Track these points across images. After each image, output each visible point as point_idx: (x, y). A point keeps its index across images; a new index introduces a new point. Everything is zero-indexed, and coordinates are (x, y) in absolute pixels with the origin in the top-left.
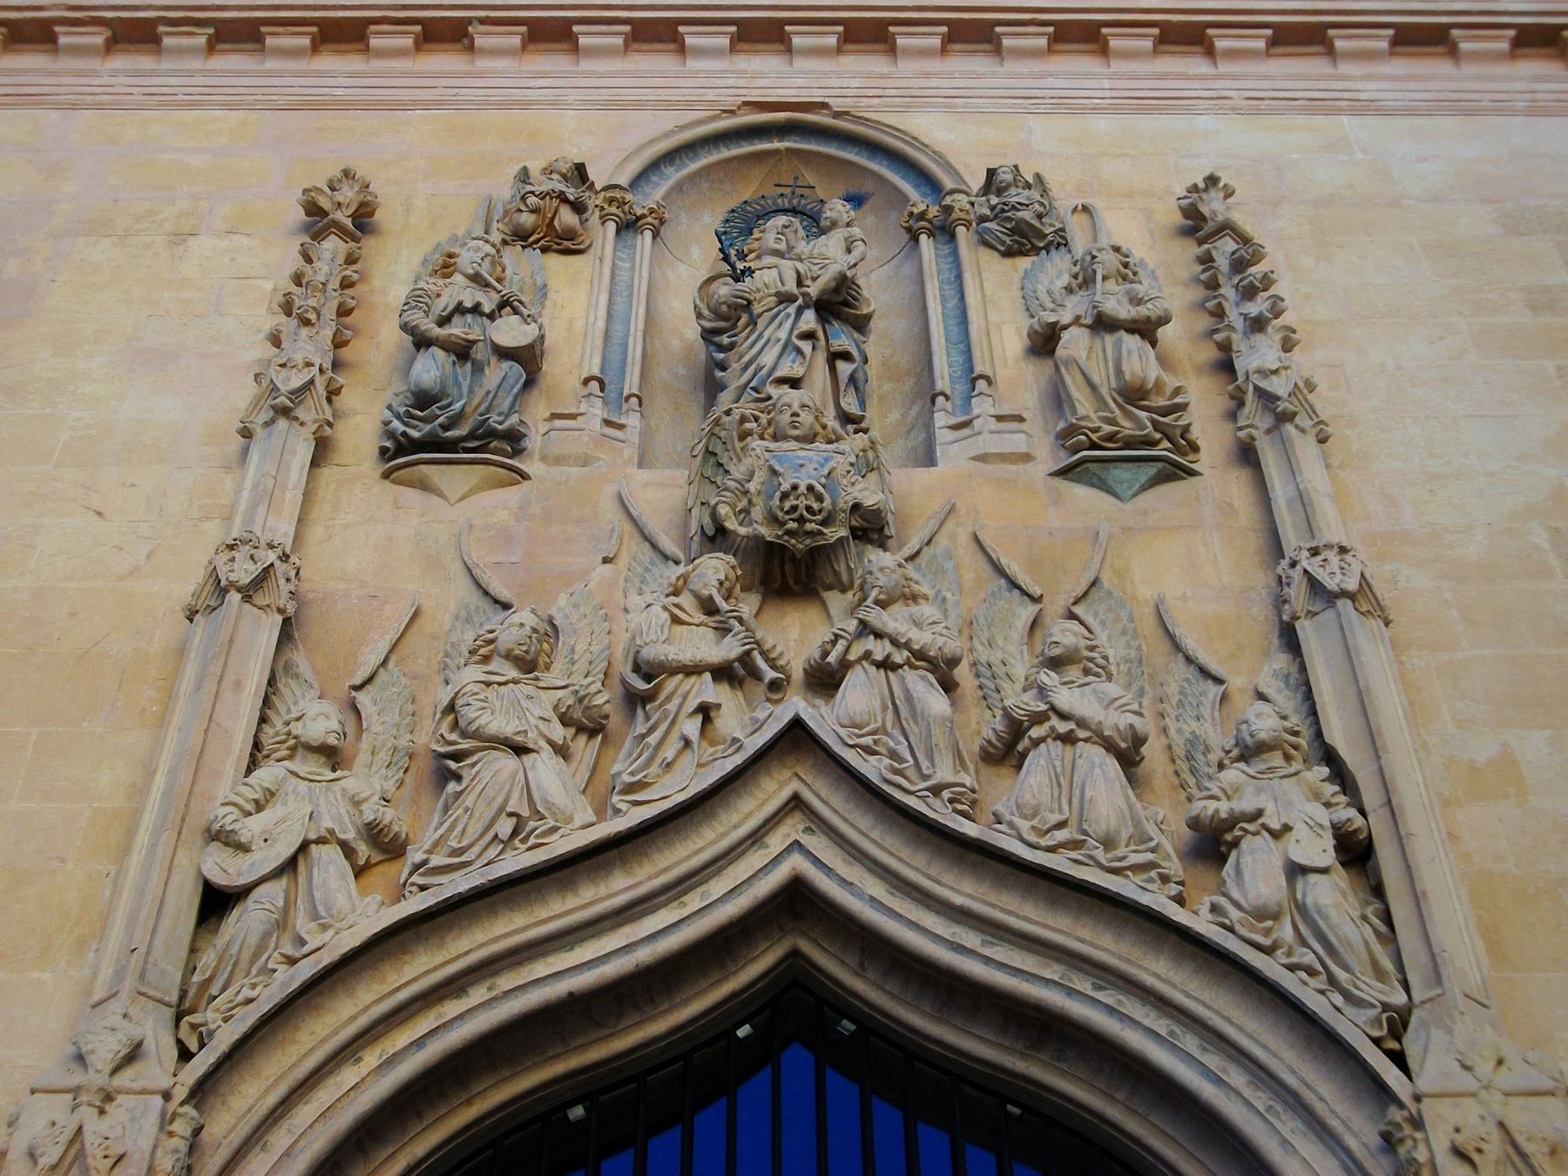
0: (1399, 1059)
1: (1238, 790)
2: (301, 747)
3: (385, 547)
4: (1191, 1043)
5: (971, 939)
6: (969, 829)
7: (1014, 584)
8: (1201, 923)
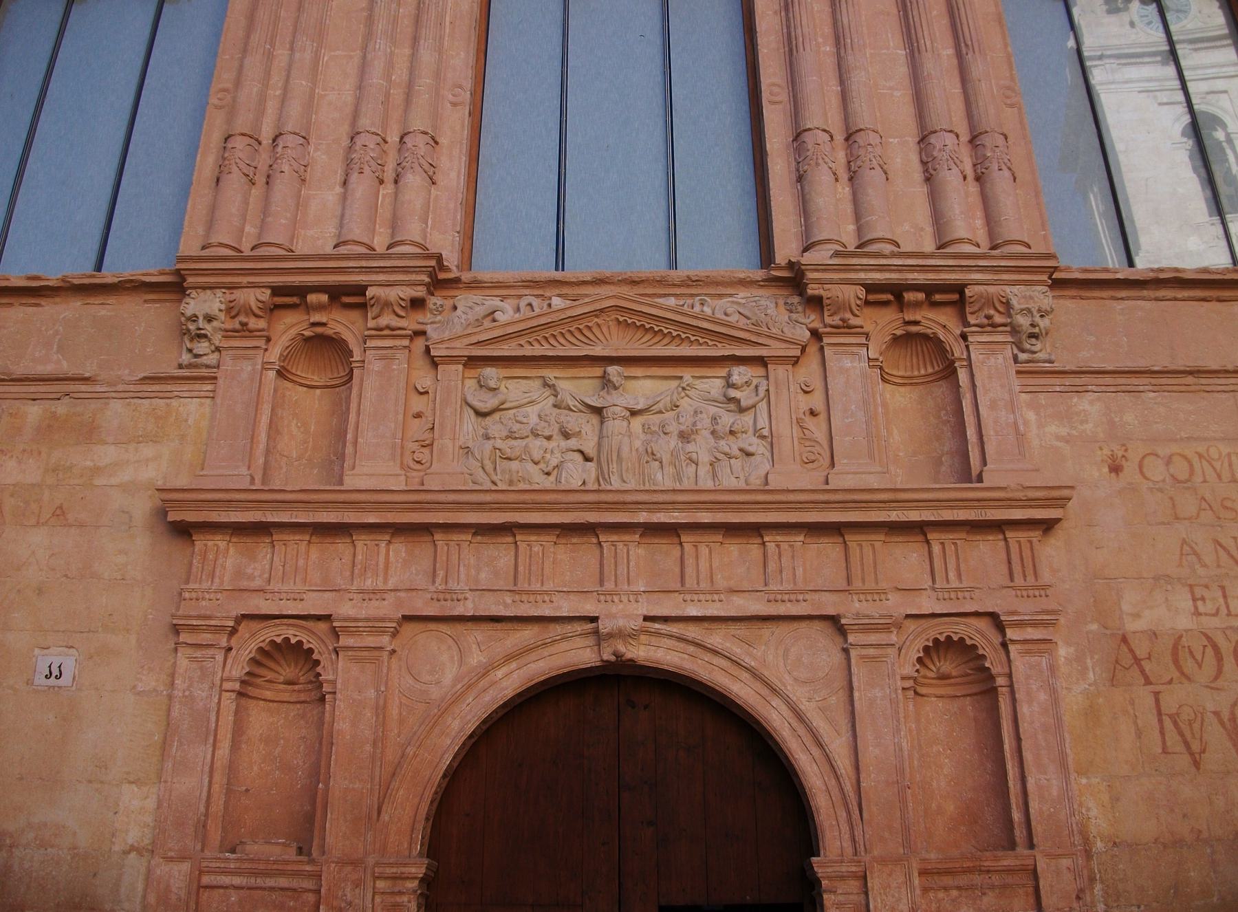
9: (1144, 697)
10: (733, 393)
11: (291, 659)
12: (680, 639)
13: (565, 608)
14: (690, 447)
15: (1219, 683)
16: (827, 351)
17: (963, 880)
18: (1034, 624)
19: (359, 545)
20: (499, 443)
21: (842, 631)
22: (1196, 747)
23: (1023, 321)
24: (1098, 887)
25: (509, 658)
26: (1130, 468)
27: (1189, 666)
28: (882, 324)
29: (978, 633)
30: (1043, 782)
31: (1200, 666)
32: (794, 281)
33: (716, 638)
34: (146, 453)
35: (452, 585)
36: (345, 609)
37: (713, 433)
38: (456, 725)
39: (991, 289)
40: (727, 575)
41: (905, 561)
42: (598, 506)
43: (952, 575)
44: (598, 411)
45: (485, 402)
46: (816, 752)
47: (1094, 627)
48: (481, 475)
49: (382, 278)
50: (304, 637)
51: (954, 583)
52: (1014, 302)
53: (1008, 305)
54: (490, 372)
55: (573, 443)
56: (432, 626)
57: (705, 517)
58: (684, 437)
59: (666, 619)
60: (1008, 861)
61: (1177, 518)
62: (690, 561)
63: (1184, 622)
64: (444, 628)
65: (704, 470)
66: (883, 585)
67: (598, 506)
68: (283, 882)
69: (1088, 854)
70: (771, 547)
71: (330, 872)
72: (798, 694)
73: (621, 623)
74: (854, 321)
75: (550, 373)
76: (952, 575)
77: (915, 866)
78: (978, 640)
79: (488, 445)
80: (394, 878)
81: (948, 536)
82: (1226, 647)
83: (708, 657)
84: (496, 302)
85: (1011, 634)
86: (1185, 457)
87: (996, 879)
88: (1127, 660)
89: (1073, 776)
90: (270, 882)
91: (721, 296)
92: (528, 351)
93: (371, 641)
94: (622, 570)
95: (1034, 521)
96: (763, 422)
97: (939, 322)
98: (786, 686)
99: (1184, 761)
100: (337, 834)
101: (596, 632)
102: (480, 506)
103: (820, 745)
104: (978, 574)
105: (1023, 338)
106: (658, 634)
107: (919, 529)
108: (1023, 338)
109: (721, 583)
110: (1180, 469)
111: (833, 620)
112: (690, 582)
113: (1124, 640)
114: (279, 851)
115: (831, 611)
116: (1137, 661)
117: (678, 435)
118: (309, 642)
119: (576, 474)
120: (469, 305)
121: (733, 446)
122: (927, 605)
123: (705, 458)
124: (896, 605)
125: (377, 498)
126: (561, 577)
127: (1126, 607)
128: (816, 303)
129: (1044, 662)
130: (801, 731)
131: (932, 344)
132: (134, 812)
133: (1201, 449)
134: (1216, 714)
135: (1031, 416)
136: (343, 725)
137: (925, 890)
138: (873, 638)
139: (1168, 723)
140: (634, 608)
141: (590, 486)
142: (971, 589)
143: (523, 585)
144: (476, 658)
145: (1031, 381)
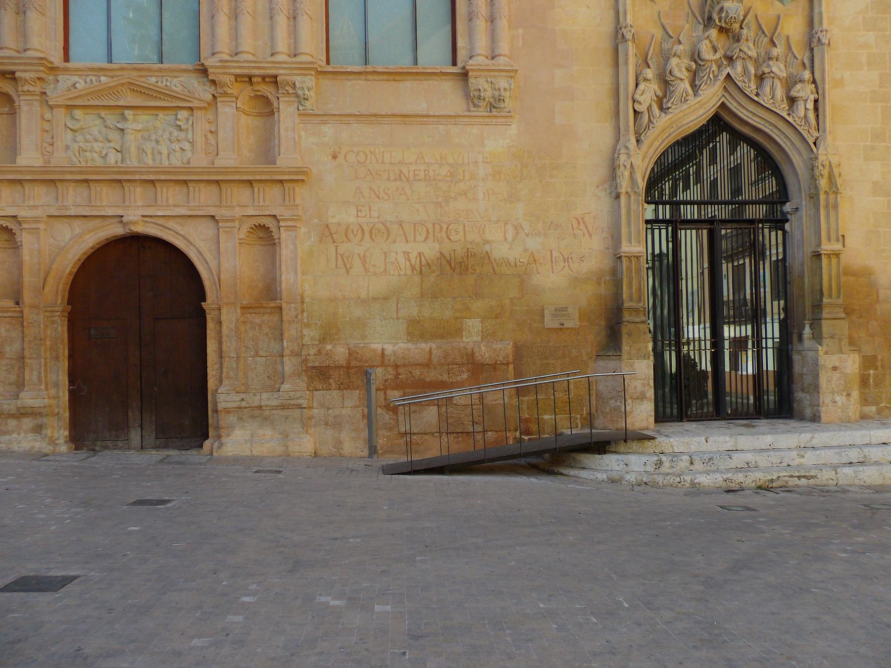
0: (815, 144)
1: (800, 91)
2: (646, 80)
4: (782, 137)
5: (750, 115)
6: (756, 98)
7: (763, 32)
8: (790, 119)
9: (332, 247)
10: (179, 123)
12: (156, 224)
13: (110, 212)
14: (159, 147)
15: (362, 243)
16: (219, 104)
17: (256, 311)
18: (290, 220)
19: (26, 188)
20: (81, 144)
21: (217, 222)
22: (348, 266)
23: (300, 92)
24: (305, 314)
25: (90, 231)
26: (341, 158)
27: (351, 236)
28: (247, 92)
29: (270, 223)
31: (355, 236)
32: (204, 71)
33: (170, 224)
35: (65, 203)
36: (22, 213)
37: (170, 140)
38: (70, 256)
39: (288, 78)
40: (172, 200)
41: (243, 194)
42: (119, 173)
43: (261, 200)
44: (122, 130)
45: (77, 126)
46: (206, 266)
47: (316, 221)
48: (74, 158)
49: (21, 68)
50: (8, 224)
51: (262, 203)
52: (297, 84)
53: (294, 84)
54: (78, 113)
55: (112, 145)
56: (60, 219)
57: (163, 177)
58: (157, 142)
59: (151, 216)
60: (272, 304)
61: (356, 178)
62: (159, 194)
64: (64, 220)
65: (164, 157)
66: (234, 204)
67: (119, 173)
68: (9, 314)
69: (302, 302)
70: (191, 188)
71: (26, 311)
73: (131, 218)
74: (229, 91)
75: (103, 113)
76: (261, 200)
77: (239, 305)
78: (270, 225)
79: (76, 145)
80: (52, 311)
81: (260, 185)
82: (366, 229)
83: (167, 231)
84: (76, 78)
85: (282, 224)
86: (365, 153)
87: (269, 310)
88: (327, 233)
89: (299, 275)
90: (5, 315)
91: (176, 77)
92: (91, 103)
93: (34, 226)
94: (132, 197)
95: (295, 179)
96: (190, 136)
97: (267, 90)
98: (194, 241)
99: (343, 271)
100: (27, 297)
101: (121, 222)
102: (71, 173)
103: (207, 263)
104: (269, 201)
105: (301, 100)
106: (147, 222)
107: (250, 182)
109: (171, 202)
110: (362, 158)
111: (213, 217)
112: (159, 202)
113: (327, 226)
115: (213, 214)
116: (331, 234)
117: (154, 141)
118: (10, 226)
119: (113, 158)
120: (65, 81)
121: (176, 146)
122: (251, 212)
123: (165, 152)
124: (238, 212)
125: (30, 170)
126: (107, 201)
127: (330, 213)
128: (213, 82)
129: (293, 234)
130: (201, 258)
133: (372, 149)
134: (359, 254)
135: (303, 134)
136: (26, 257)
137: (243, 314)
138: (228, 224)
139: (339, 258)
141: (119, 164)
142: (268, 206)
143: (93, 203)
144: (77, 231)
145: (304, 118)
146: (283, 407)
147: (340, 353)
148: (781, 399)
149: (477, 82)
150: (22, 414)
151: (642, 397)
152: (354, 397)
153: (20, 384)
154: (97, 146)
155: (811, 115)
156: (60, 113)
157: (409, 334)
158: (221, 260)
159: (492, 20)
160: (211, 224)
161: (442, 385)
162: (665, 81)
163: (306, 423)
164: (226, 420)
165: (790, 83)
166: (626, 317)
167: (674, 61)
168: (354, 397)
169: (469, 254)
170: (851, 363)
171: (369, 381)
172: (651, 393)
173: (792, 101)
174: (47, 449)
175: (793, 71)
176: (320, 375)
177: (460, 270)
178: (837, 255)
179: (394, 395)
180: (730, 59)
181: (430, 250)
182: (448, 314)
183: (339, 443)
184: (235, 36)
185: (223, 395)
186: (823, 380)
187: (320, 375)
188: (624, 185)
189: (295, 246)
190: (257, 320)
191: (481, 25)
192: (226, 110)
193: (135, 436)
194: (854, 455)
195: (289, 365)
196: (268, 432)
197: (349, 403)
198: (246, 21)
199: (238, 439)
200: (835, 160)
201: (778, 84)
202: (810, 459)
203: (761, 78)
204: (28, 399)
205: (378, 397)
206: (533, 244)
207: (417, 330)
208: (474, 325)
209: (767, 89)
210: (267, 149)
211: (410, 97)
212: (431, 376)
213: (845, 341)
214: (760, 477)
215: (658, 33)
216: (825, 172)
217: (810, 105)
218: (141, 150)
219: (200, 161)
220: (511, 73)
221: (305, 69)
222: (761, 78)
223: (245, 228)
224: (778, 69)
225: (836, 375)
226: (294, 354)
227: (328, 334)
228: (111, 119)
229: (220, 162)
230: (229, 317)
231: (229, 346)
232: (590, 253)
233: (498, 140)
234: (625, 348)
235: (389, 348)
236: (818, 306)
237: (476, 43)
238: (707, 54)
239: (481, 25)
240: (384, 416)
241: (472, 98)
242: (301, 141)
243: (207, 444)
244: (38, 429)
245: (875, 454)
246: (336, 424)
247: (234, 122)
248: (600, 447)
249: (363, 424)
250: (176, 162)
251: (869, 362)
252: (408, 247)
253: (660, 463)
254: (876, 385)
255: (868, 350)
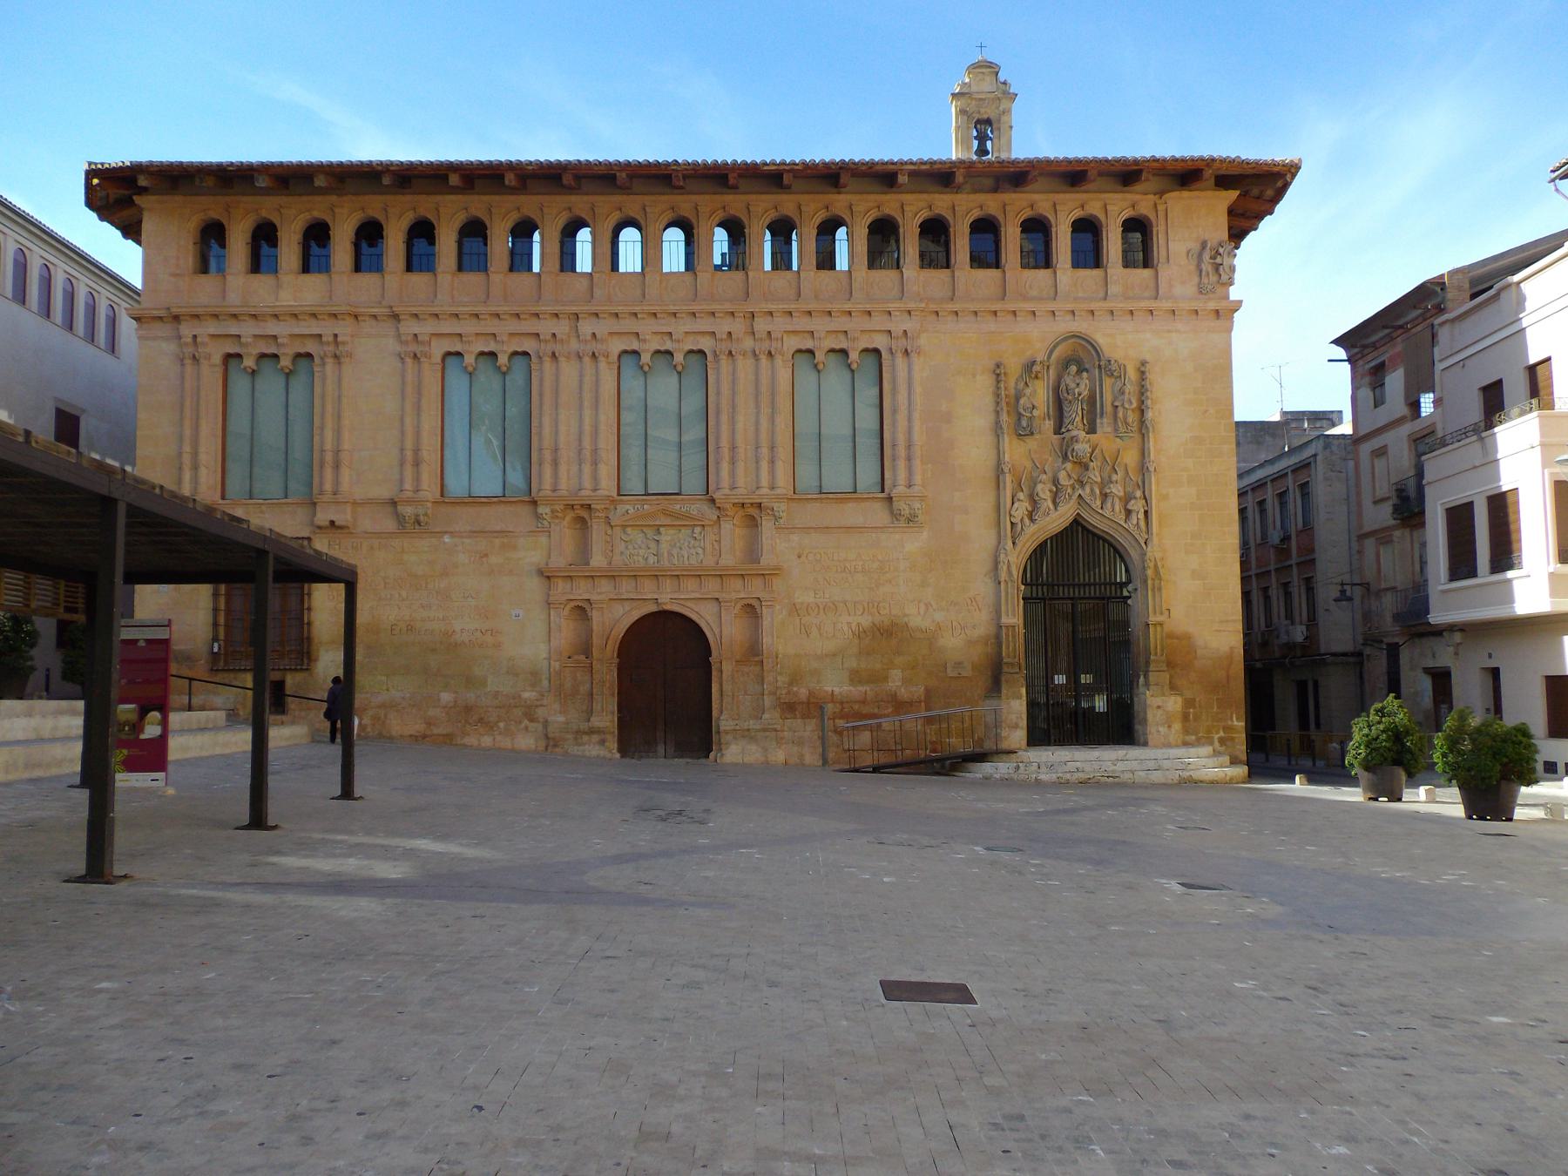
3: (1016, 452)
11: (581, 612)
28: (741, 513)
29: (755, 603)
30: (767, 640)
32: (713, 501)
34: (531, 554)
36: (593, 597)
40: (690, 588)
41: (738, 583)
54: (629, 530)
63: (811, 600)
72: (708, 618)
95: (776, 572)
97: (754, 512)
98: (704, 616)
104: (756, 589)
105: (776, 519)
108: (776, 519)
114: (582, 657)
119: (652, 560)
120: (621, 509)
124: (734, 596)
126: (648, 590)
131: (752, 518)
132: (542, 651)
140: (669, 598)
146: (764, 730)
147: (803, 693)
148: (1121, 727)
149: (899, 505)
150: (592, 731)
151: (1016, 726)
152: (812, 724)
153: (590, 712)
154: (642, 552)
155: (1142, 523)
156: (618, 530)
157: (851, 680)
158: (723, 629)
159: (909, 459)
160: (715, 604)
161: (874, 716)
162: (1034, 500)
163: (780, 741)
164: (725, 738)
165: (1127, 498)
166: (1005, 669)
167: (1039, 487)
168: (812, 724)
169: (893, 624)
170: (1174, 704)
171: (822, 715)
172: (1024, 723)
173: (1128, 513)
174: (609, 755)
175: (1129, 489)
176: (789, 708)
177: (887, 635)
178: (1161, 624)
179: (841, 723)
180: (1082, 484)
181: (866, 621)
182: (878, 666)
183: (801, 756)
184: (733, 474)
185: (724, 721)
186: (1150, 716)
187: (789, 708)
188: (1003, 576)
189: (772, 618)
190: (746, 669)
191: (901, 464)
192: (726, 526)
193: (661, 749)
194: (1152, 765)
195: (768, 701)
196: (753, 747)
197: (809, 728)
198: (740, 466)
199: (733, 752)
200: (1158, 555)
201: (1117, 501)
202: (1120, 766)
203: (1105, 496)
204: (596, 722)
205: (829, 724)
206: (939, 616)
207: (855, 677)
208: (896, 676)
209: (1109, 505)
210: (753, 552)
211: (852, 514)
212: (865, 710)
213: (1166, 687)
214: (1082, 776)
215: (1029, 465)
216: (1152, 565)
217: (1141, 516)
218: (670, 554)
219: (709, 561)
220: (922, 498)
221: (780, 498)
222: (1105, 496)
223: (739, 606)
224: (1117, 490)
225: (1160, 712)
226: (770, 693)
227: (795, 679)
228: (650, 533)
229: (723, 562)
230: (727, 667)
231: (727, 687)
232: (979, 623)
233: (914, 543)
234: (1004, 691)
235: (837, 690)
236: (1148, 663)
237: (898, 475)
238: (1063, 479)
239: (901, 464)
240: (834, 738)
241: (895, 515)
242: (777, 546)
243: (712, 755)
244: (602, 742)
245: (1166, 764)
246: (800, 742)
247: (732, 533)
248: (981, 757)
249: (818, 743)
250: (693, 561)
251: (1189, 703)
252: (850, 619)
253: (1018, 768)
254: (1195, 720)
255: (1189, 694)
